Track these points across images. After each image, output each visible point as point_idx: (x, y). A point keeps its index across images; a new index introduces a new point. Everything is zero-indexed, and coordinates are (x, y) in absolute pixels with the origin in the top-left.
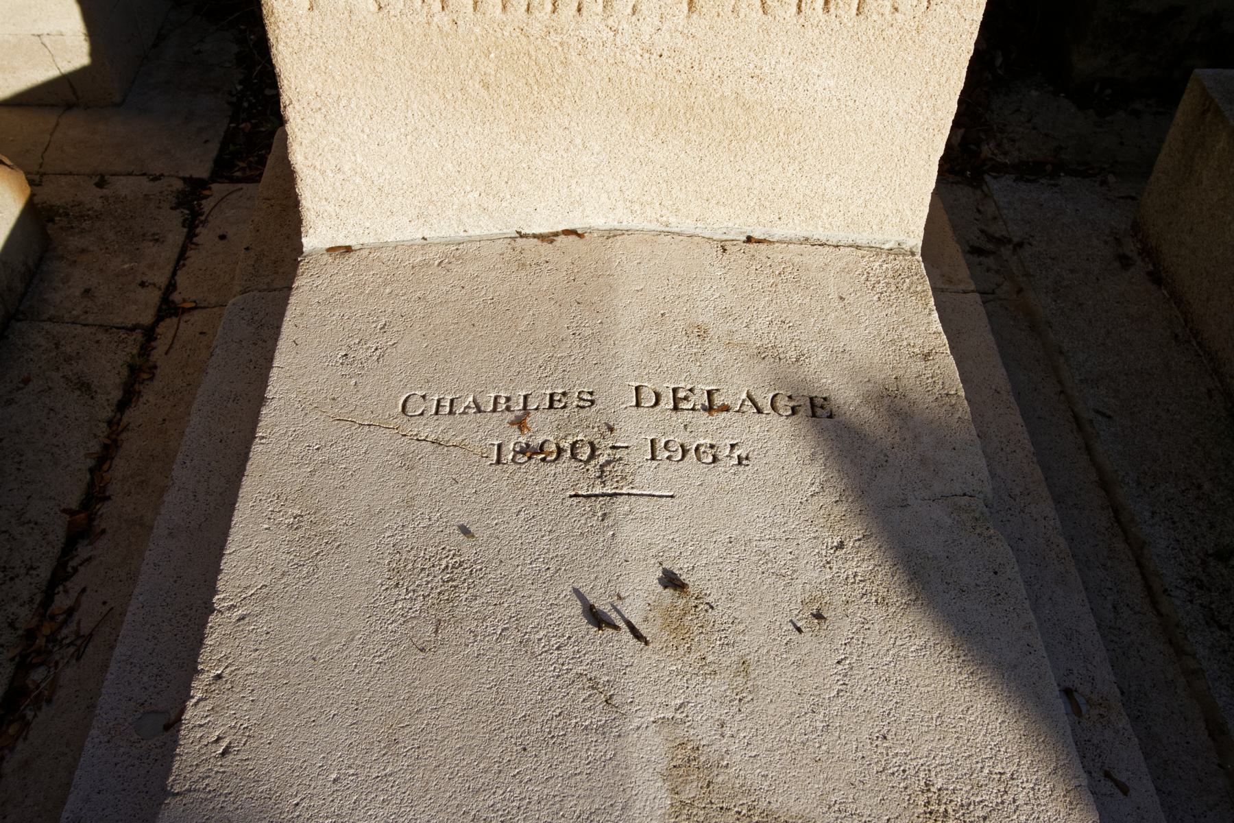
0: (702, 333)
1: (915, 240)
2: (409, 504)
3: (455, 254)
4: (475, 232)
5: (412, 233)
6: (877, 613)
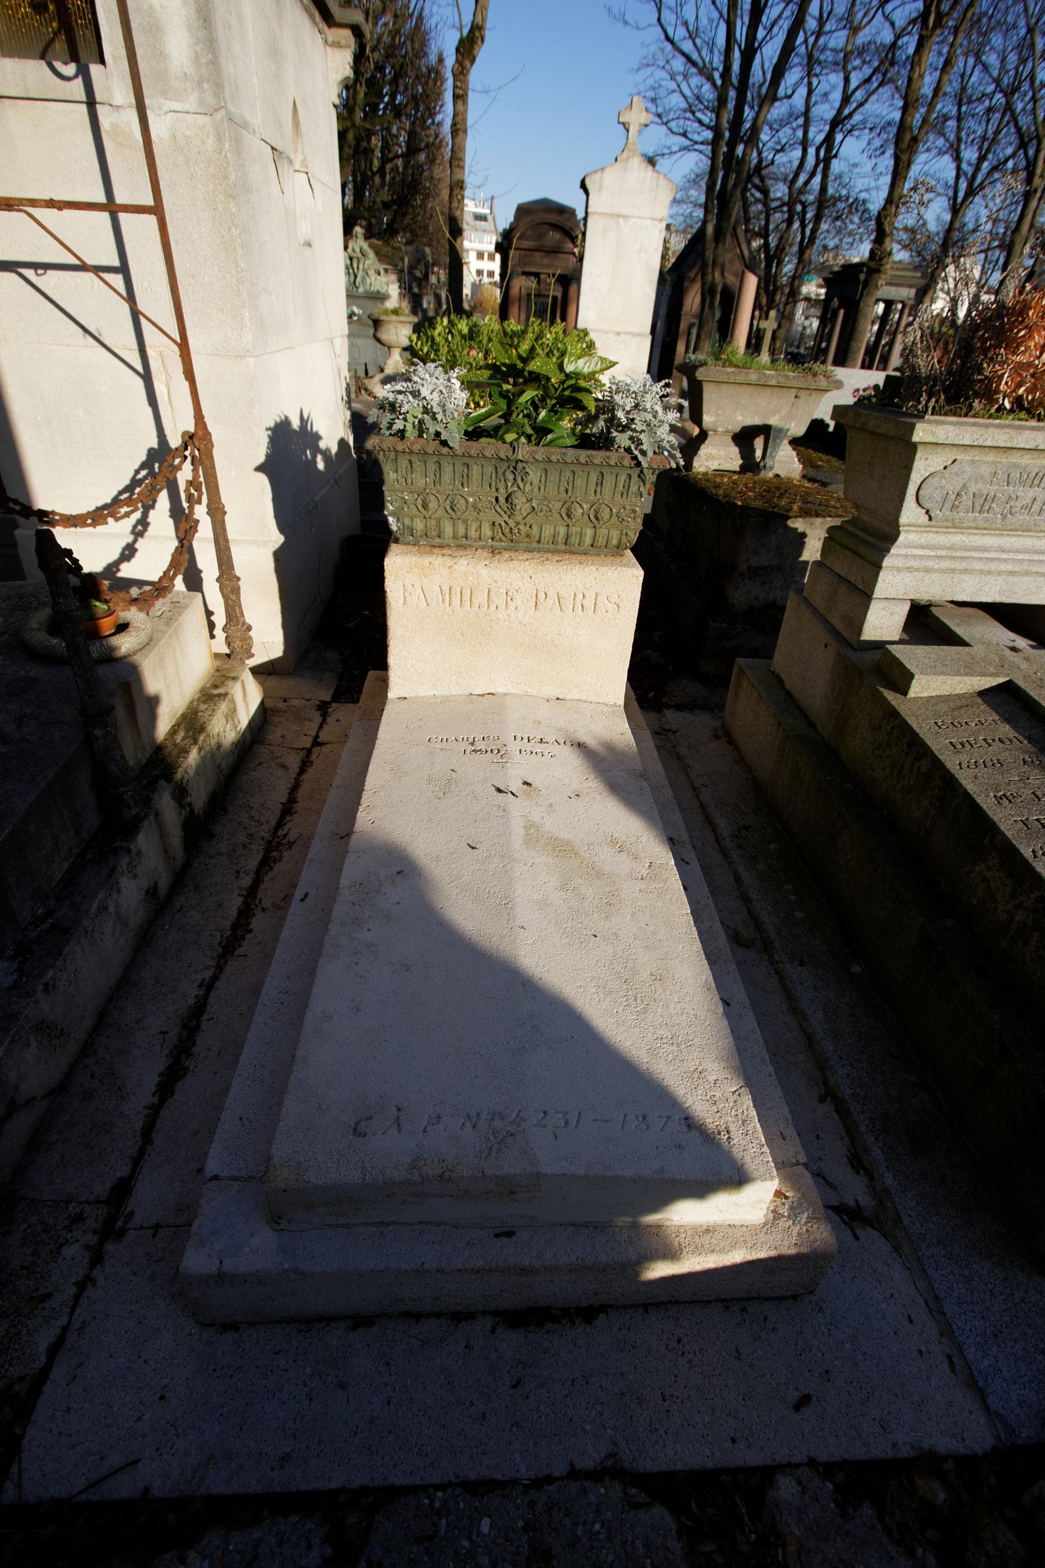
0: (539, 723)
1: (621, 702)
2: (433, 764)
3: (446, 700)
4: (454, 693)
5: (430, 692)
6: (599, 797)
